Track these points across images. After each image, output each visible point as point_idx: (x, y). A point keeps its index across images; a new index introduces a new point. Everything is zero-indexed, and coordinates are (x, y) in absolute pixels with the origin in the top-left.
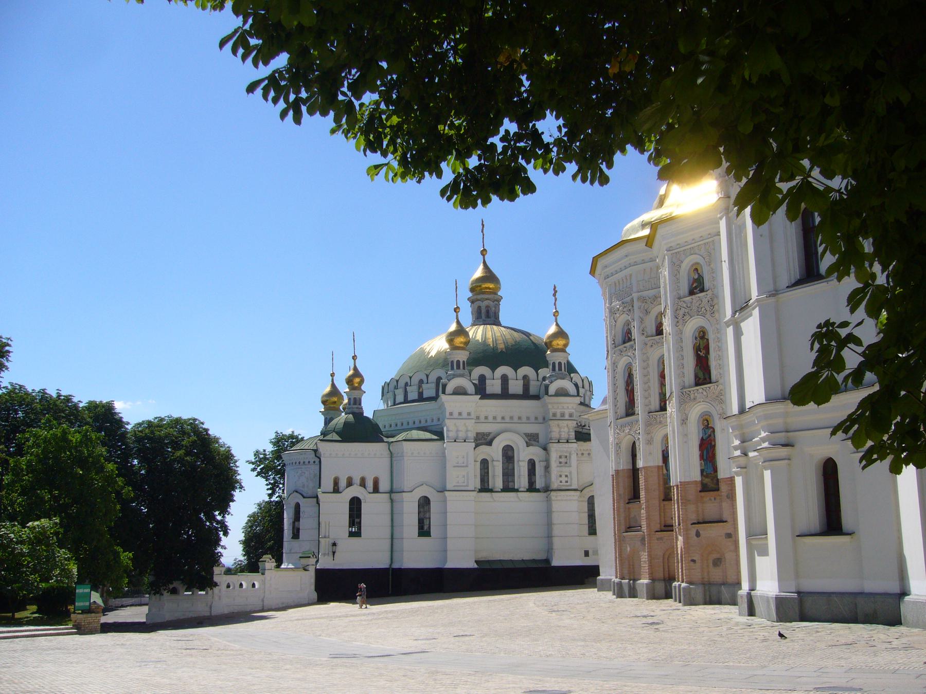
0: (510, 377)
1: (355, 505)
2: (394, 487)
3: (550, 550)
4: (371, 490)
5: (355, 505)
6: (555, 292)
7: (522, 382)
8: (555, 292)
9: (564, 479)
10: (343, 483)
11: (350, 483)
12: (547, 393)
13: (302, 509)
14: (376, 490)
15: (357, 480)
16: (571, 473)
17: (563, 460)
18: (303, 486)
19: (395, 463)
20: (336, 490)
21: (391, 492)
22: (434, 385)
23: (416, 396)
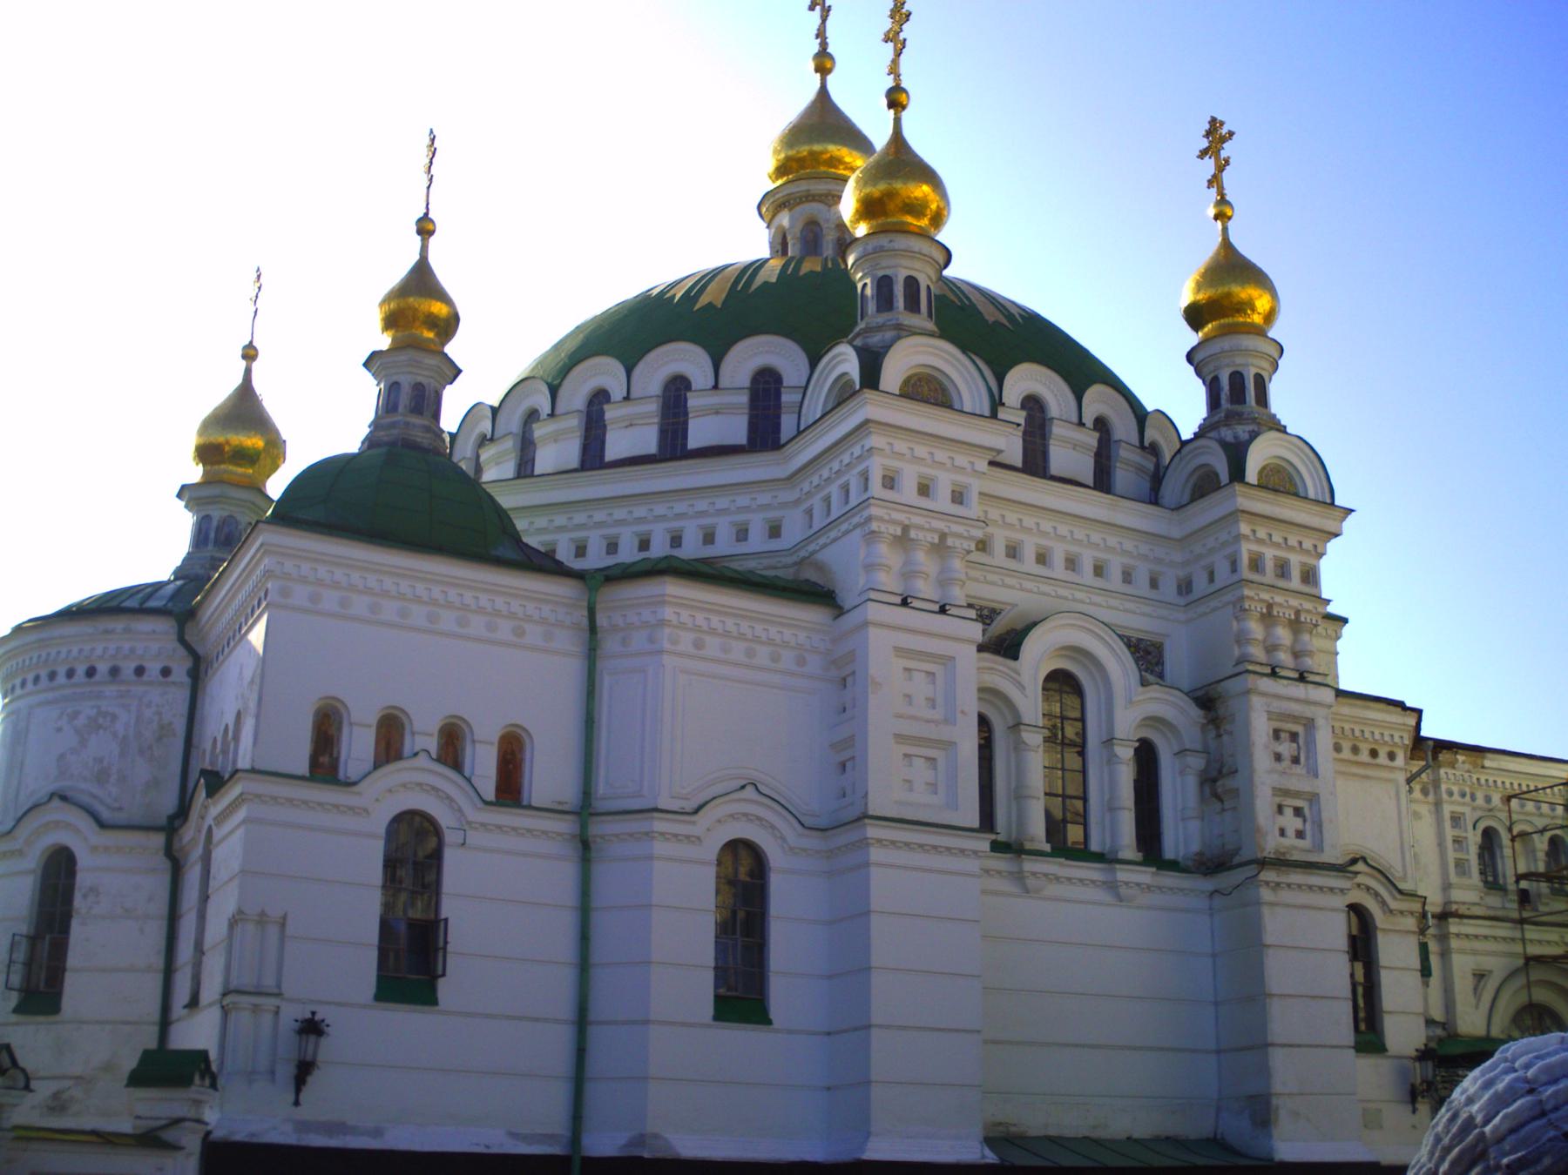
0: (1054, 410)
1: (414, 854)
2: (601, 788)
3: (1261, 1111)
4: (489, 792)
5: (414, 854)
6: (1217, 135)
7: (1091, 439)
8: (1217, 135)
9: (1291, 822)
10: (358, 746)
11: (391, 738)
12: (1238, 473)
13: (83, 879)
14: (510, 789)
15: (423, 737)
16: (1313, 798)
17: (1286, 748)
18: (102, 777)
19: (606, 682)
20: (325, 763)
21: (585, 809)
22: (744, 399)
23: (646, 439)
